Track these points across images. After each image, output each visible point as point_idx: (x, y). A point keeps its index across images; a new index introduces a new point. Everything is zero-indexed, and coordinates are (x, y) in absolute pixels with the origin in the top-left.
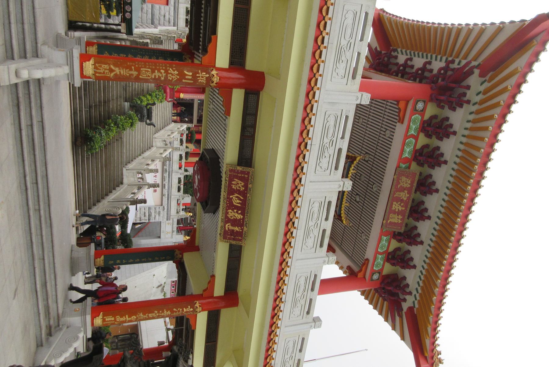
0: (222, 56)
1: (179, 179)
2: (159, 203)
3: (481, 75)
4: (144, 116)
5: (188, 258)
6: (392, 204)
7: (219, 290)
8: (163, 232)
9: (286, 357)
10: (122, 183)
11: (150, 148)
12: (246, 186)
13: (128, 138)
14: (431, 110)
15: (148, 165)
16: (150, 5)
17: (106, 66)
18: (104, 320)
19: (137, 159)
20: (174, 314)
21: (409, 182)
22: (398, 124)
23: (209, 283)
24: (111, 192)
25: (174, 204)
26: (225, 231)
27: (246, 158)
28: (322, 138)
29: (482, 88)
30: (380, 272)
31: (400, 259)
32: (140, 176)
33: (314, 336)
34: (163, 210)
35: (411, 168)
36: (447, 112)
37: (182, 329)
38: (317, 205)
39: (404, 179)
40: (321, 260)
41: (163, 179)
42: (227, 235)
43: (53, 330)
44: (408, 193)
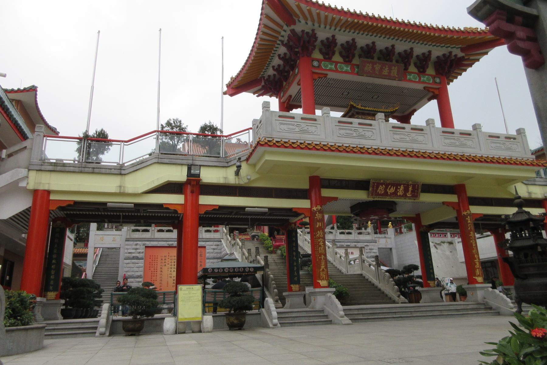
0: (303, 204)
3: (294, 24)
5: (426, 222)
6: (384, 75)
7: (453, 198)
9: (503, 148)
10: (361, 275)
12: (382, 184)
14: (317, 55)
16: (207, 261)
17: (321, 273)
18: (479, 276)
20: (472, 229)
21: (368, 64)
22: (328, 77)
23: (448, 206)
24: (370, 282)
25: (361, 237)
26: (412, 196)
27: (361, 185)
28: (353, 137)
29: (303, 21)
30: (434, 77)
31: (423, 63)
32: (352, 262)
33: (487, 129)
34: (368, 246)
35: (358, 63)
36: (318, 43)
37: (482, 224)
38: (395, 136)
39: (366, 69)
40: (432, 129)
41: (342, 247)
42: (415, 195)
43: (487, 307)
44: (376, 64)
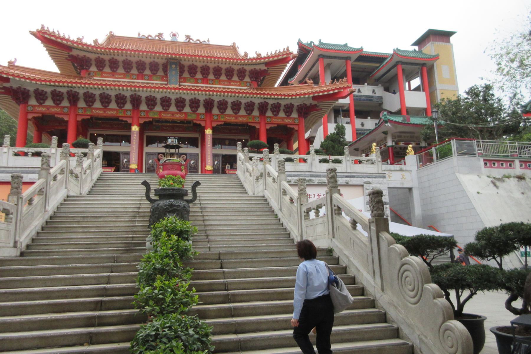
1: (321, 161)
2: (360, 189)
4: (172, 206)
8: (403, 184)
11: (266, 200)
13: (237, 238)
15: (292, 201)
19: (283, 220)
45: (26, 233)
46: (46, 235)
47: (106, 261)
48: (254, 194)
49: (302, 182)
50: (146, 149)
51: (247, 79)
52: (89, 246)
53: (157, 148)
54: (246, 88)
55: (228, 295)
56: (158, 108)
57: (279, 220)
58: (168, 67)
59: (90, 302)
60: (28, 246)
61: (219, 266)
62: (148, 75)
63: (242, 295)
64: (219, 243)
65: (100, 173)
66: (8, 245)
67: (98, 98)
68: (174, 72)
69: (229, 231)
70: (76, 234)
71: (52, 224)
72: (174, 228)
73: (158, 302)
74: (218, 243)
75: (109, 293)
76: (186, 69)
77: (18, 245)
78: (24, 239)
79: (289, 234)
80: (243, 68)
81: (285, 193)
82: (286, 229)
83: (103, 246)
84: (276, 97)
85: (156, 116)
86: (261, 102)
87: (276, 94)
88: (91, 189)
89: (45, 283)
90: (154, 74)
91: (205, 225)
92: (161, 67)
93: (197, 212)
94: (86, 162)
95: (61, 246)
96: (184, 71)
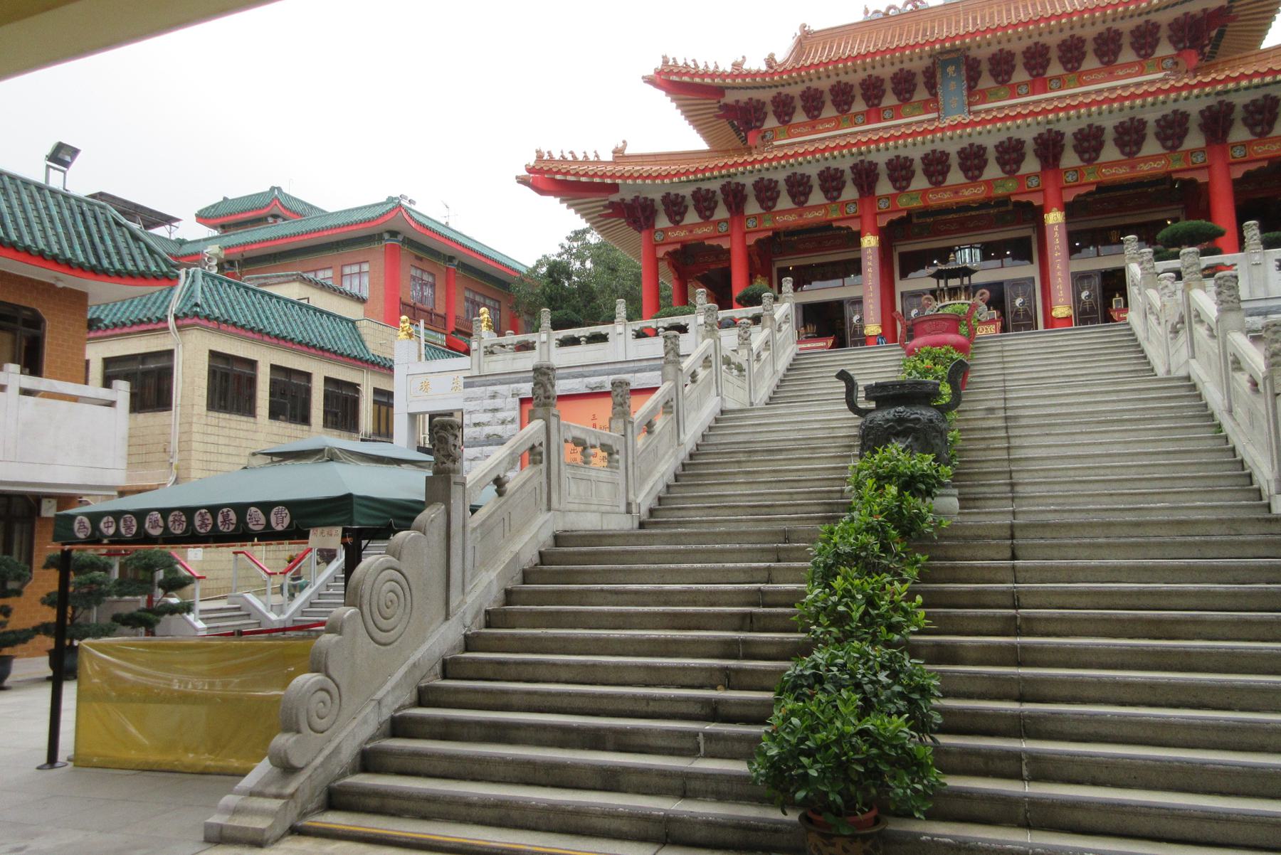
4: (900, 420)
11: (1194, 387)
45: (647, 488)
46: (683, 490)
47: (768, 539)
48: (1169, 372)
49: (1275, 333)
50: (902, 286)
51: (1165, 49)
52: (756, 510)
53: (922, 281)
54: (1160, 75)
55: (1014, 618)
56: (920, 182)
57: (1226, 438)
58: (939, 76)
59: (732, 615)
60: (652, 512)
61: (1009, 554)
62: (891, 108)
63: (1048, 620)
64: (1040, 501)
65: (793, 355)
66: (617, 510)
67: (783, 187)
68: (953, 83)
69: (1072, 473)
70: (733, 487)
71: (692, 470)
72: (893, 470)
73: (840, 619)
74: (1037, 501)
75: (768, 599)
76: (985, 67)
77: (634, 510)
78: (644, 499)
79: (1250, 476)
80: (1147, 22)
81: (1237, 365)
82: (1242, 462)
83: (782, 509)
84: (1256, 81)
85: (917, 204)
86: (1209, 108)
87: (1256, 74)
88: (774, 392)
89: (664, 577)
90: (905, 101)
91: (1009, 460)
92: (920, 80)
93: (993, 428)
94: (758, 336)
95: (707, 511)
96: (979, 74)
